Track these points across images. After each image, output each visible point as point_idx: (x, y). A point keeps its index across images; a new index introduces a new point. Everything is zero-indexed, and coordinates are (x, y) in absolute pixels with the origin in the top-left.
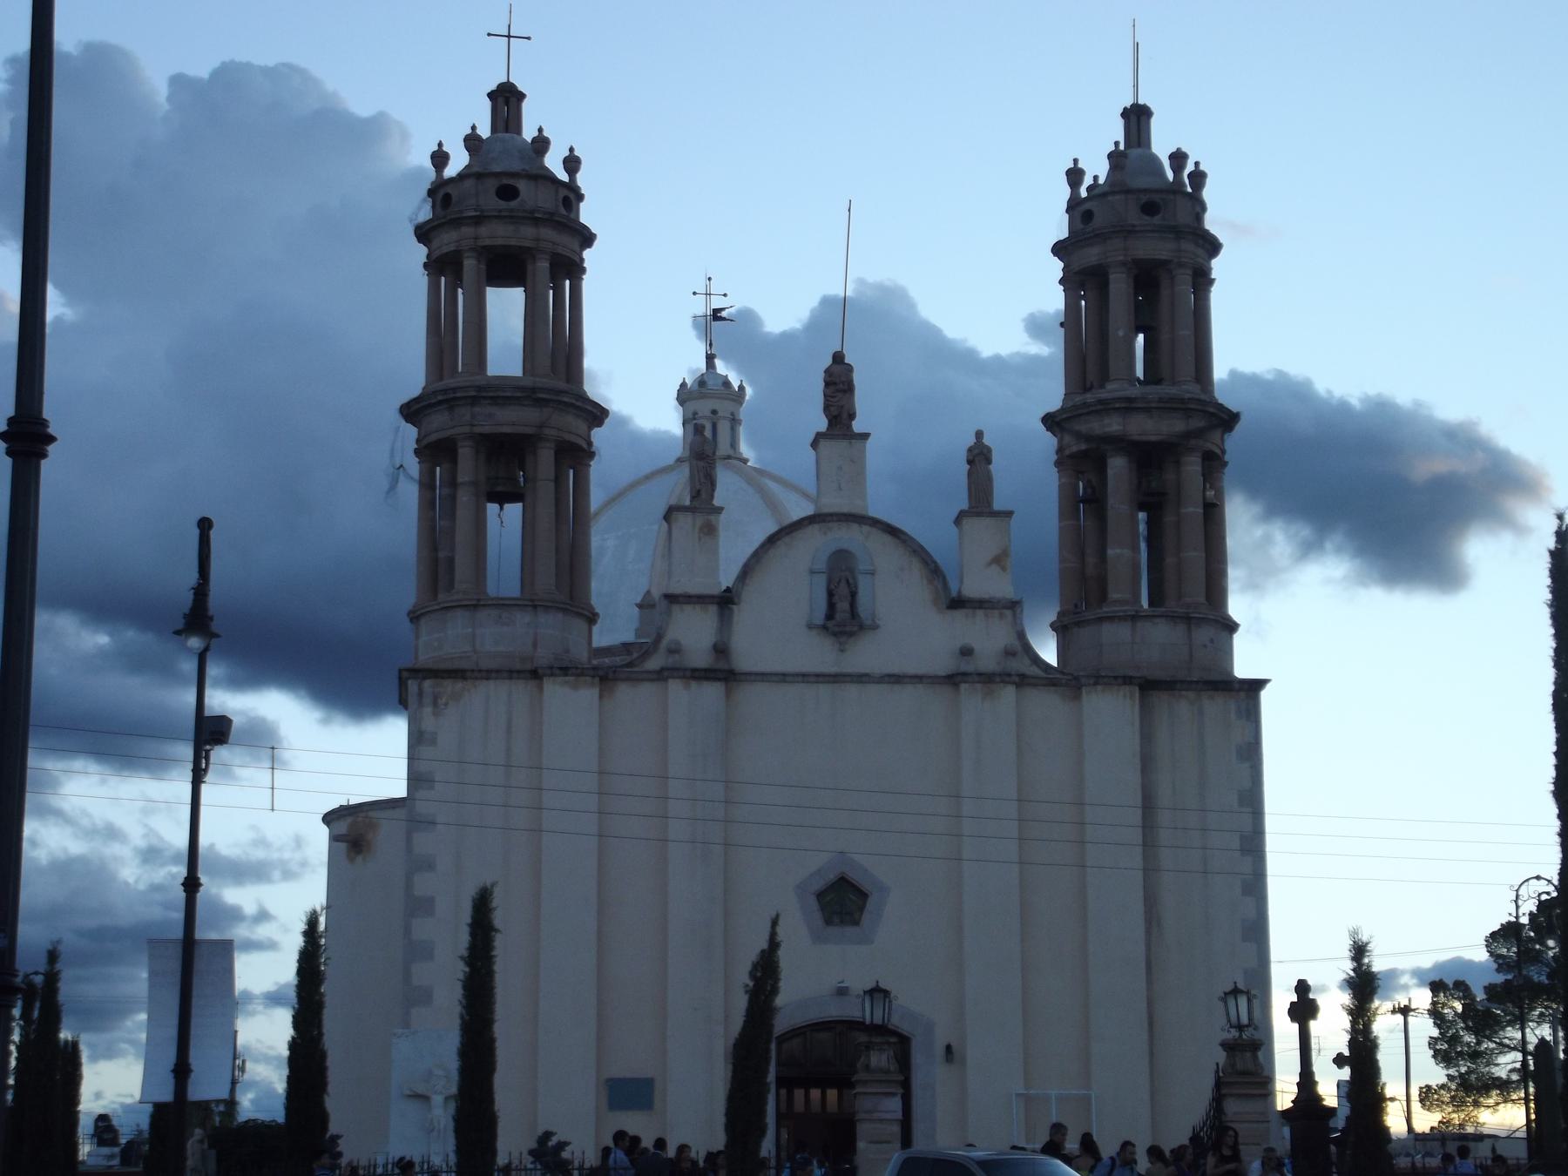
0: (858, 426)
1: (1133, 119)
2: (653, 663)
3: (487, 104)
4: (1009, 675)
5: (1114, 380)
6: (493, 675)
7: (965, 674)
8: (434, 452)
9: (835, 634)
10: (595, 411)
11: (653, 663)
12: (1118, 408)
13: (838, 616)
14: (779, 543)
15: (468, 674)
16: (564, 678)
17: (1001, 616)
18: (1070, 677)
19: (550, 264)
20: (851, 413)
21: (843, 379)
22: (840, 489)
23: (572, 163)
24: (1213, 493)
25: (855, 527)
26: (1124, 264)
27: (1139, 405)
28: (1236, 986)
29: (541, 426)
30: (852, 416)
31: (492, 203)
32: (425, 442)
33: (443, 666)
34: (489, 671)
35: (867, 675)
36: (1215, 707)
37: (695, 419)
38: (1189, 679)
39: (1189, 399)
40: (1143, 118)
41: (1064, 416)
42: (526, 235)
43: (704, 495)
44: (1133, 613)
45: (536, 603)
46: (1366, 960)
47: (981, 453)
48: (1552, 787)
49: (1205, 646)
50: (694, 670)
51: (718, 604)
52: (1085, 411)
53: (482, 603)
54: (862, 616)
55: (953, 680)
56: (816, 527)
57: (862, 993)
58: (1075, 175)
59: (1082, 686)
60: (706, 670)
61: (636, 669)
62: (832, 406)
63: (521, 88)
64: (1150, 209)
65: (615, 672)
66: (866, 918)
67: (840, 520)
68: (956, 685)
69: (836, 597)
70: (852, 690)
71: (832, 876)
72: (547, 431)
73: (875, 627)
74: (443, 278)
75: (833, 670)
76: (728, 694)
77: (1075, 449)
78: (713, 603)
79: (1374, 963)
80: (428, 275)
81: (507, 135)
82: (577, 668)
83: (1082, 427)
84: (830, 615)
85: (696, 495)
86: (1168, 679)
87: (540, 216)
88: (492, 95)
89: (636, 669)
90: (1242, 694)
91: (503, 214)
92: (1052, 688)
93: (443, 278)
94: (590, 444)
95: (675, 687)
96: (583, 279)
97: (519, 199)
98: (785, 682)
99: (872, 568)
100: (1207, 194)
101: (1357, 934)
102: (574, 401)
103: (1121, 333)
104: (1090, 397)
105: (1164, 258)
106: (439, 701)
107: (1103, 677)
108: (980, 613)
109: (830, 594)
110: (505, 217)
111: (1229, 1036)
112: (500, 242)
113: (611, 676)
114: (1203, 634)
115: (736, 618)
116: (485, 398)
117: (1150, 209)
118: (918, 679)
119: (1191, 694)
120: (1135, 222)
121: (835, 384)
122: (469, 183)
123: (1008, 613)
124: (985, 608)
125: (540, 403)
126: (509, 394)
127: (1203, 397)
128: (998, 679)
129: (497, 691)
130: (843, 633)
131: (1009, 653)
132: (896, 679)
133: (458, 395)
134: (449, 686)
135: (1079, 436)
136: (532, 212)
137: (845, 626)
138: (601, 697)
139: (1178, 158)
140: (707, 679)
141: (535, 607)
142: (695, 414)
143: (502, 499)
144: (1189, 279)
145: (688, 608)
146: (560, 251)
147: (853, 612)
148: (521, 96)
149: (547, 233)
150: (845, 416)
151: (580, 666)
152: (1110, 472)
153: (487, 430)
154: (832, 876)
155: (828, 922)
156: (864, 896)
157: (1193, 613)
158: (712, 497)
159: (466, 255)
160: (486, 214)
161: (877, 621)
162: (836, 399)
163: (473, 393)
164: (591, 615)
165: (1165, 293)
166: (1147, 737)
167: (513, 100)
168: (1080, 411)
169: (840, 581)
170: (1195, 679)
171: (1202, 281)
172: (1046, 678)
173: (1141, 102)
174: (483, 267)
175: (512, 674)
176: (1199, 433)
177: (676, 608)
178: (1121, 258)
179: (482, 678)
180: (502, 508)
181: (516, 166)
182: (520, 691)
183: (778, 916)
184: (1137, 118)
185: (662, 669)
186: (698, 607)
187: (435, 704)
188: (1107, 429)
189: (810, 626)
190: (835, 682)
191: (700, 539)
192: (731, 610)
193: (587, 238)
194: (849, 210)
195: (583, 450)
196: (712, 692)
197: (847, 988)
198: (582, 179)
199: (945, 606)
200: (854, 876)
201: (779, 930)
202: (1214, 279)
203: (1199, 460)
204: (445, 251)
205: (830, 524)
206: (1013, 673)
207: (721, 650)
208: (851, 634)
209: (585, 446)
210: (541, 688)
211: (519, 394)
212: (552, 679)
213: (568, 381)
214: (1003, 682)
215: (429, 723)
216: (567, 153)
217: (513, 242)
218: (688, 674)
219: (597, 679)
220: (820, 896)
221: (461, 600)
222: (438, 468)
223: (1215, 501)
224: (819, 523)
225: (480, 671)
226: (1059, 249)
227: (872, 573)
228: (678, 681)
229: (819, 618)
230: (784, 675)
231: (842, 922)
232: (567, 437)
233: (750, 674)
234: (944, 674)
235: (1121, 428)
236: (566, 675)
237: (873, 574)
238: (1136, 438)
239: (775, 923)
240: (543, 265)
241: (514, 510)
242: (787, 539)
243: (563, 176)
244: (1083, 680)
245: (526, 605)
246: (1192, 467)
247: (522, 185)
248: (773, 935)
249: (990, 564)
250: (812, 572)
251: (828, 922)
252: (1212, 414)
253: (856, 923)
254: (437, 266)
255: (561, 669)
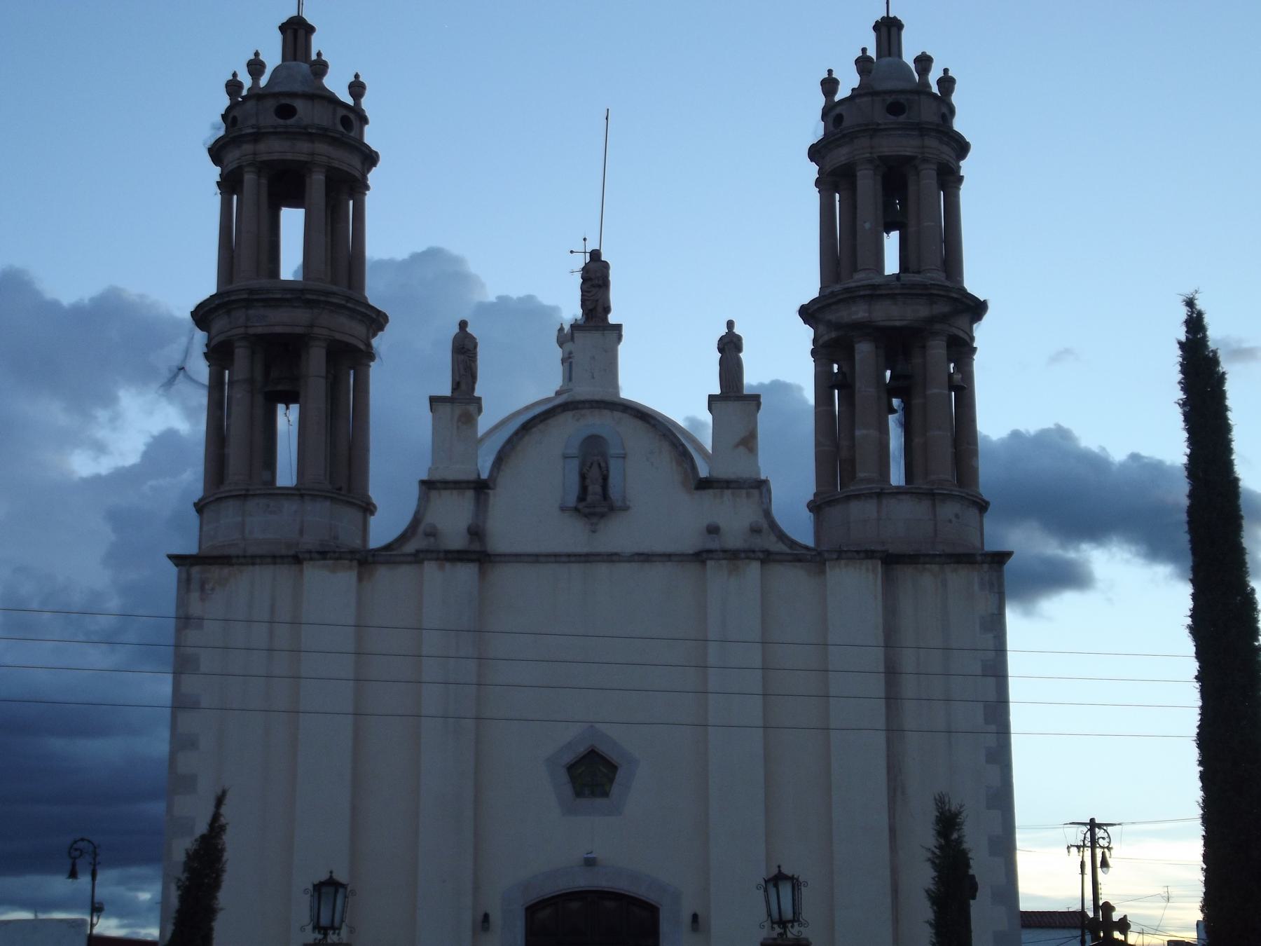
0: (613, 319)
1: (884, 30)
2: (410, 548)
3: (278, 38)
4: (754, 552)
5: (860, 270)
6: (258, 560)
7: (709, 551)
8: (218, 355)
9: (586, 516)
10: (368, 313)
11: (410, 548)
12: (864, 296)
13: (590, 498)
14: (534, 430)
15: (234, 560)
16: (322, 562)
17: (748, 495)
18: (814, 553)
19: (326, 177)
20: (606, 306)
21: (598, 275)
22: (593, 378)
23: (357, 88)
24: (960, 376)
25: (607, 413)
26: (870, 161)
27: (884, 292)
28: (780, 871)
29: (312, 326)
30: (607, 310)
31: (269, 120)
32: (213, 343)
33: (215, 553)
34: (253, 557)
35: (616, 554)
36: (958, 578)
37: (570, 358)
38: (931, 552)
39: (931, 284)
40: (894, 30)
41: (816, 307)
42: (302, 150)
43: (463, 387)
44: (878, 490)
45: (303, 492)
46: (955, 836)
47: (731, 341)
48: (1189, 621)
49: (950, 521)
50: (447, 552)
51: (475, 489)
52: (834, 300)
53: (251, 493)
54: (612, 498)
55: (700, 557)
56: (567, 417)
57: (311, 888)
58: (829, 85)
59: (825, 561)
60: (458, 552)
61: (392, 553)
62: (588, 300)
63: (310, 21)
64: (895, 109)
65: (374, 555)
66: (615, 789)
67: (592, 407)
68: (703, 562)
69: (588, 481)
70: (603, 569)
71: (582, 749)
72: (316, 330)
73: (626, 508)
74: (235, 197)
75: (585, 550)
76: (482, 574)
77: (826, 338)
78: (469, 488)
79: (965, 839)
80: (221, 193)
81: (294, 63)
82: (335, 552)
83: (832, 317)
84: (582, 497)
85: (456, 386)
86: (912, 553)
87: (314, 131)
88: (283, 28)
89: (392, 553)
90: (986, 567)
91: (279, 130)
92: (798, 564)
93: (235, 197)
94: (369, 345)
95: (430, 568)
96: (365, 194)
97: (297, 116)
98: (537, 562)
99: (623, 452)
100: (956, 99)
101: (943, 803)
102: (343, 302)
103: (867, 226)
104: (837, 288)
105: (908, 154)
106: (207, 587)
107: (846, 552)
108: (728, 493)
109: (583, 477)
110: (280, 133)
111: (774, 935)
112: (275, 157)
113: (370, 559)
114: (948, 510)
115: (492, 500)
116: (257, 300)
117: (895, 109)
118: (668, 557)
119: (935, 568)
120: (880, 122)
121: (591, 279)
122: (250, 104)
123: (755, 492)
124: (734, 488)
125: (310, 304)
126: (279, 296)
127: (948, 284)
128: (743, 555)
129: (263, 576)
130: (594, 514)
131: (755, 530)
132: (645, 558)
133: (233, 298)
134: (215, 572)
135: (832, 326)
136: (306, 128)
137: (594, 507)
138: (360, 579)
139: (924, 62)
140: (461, 560)
141: (302, 496)
142: (570, 353)
143: (289, 398)
144: (934, 173)
145: (446, 494)
146: (337, 166)
147: (605, 495)
148: (310, 29)
149: (322, 148)
150: (600, 309)
151: (337, 550)
152: (857, 357)
153: (260, 330)
154: (582, 750)
155: (579, 794)
156: (613, 768)
157: (938, 489)
158: (473, 389)
159: (246, 169)
160: (263, 131)
161: (628, 503)
162: (592, 293)
163: (245, 296)
164: (364, 505)
165: (912, 188)
166: (891, 612)
167: (301, 33)
168: (830, 301)
169: (592, 464)
170: (938, 553)
171: (950, 180)
172: (791, 554)
173: (891, 15)
174: (264, 181)
175: (275, 559)
176: (944, 318)
177: (434, 494)
178: (868, 155)
179: (247, 564)
180: (287, 408)
181: (297, 87)
182: (284, 573)
183: (224, 793)
184: (888, 29)
185: (418, 552)
186: (455, 492)
187: (202, 588)
188: (854, 317)
189: (563, 509)
190: (586, 562)
191: (458, 428)
192: (487, 494)
193: (371, 159)
194: (607, 119)
195: (360, 350)
196: (466, 573)
197: (594, 858)
198: (365, 103)
199: (693, 487)
200: (603, 749)
201: (223, 810)
202: (963, 177)
203: (945, 344)
204: (231, 168)
205: (583, 412)
206: (757, 549)
207: (476, 533)
208: (602, 516)
209: (362, 347)
210: (301, 571)
211: (288, 296)
212: (311, 563)
213: (350, 287)
214: (748, 558)
215: (196, 608)
216: (353, 79)
217: (289, 157)
218: (442, 555)
219: (355, 563)
220: (571, 768)
221: (230, 491)
222: (227, 372)
223: (962, 384)
224: (573, 410)
225: (245, 557)
226: (815, 153)
227: (624, 457)
228: (433, 562)
229: (572, 500)
230: (537, 555)
231: (593, 794)
232: (338, 336)
233: (505, 555)
234: (691, 552)
235: (867, 315)
236: (325, 559)
237: (624, 458)
238: (882, 324)
239: (219, 801)
240: (317, 181)
241: (295, 409)
242: (541, 426)
243: (350, 101)
244: (826, 555)
245: (292, 495)
246: (937, 349)
247: (299, 104)
248: (216, 817)
249: (737, 446)
250: (565, 457)
251: (579, 794)
252: (956, 300)
253: (605, 794)
254: (229, 185)
255: (319, 552)
